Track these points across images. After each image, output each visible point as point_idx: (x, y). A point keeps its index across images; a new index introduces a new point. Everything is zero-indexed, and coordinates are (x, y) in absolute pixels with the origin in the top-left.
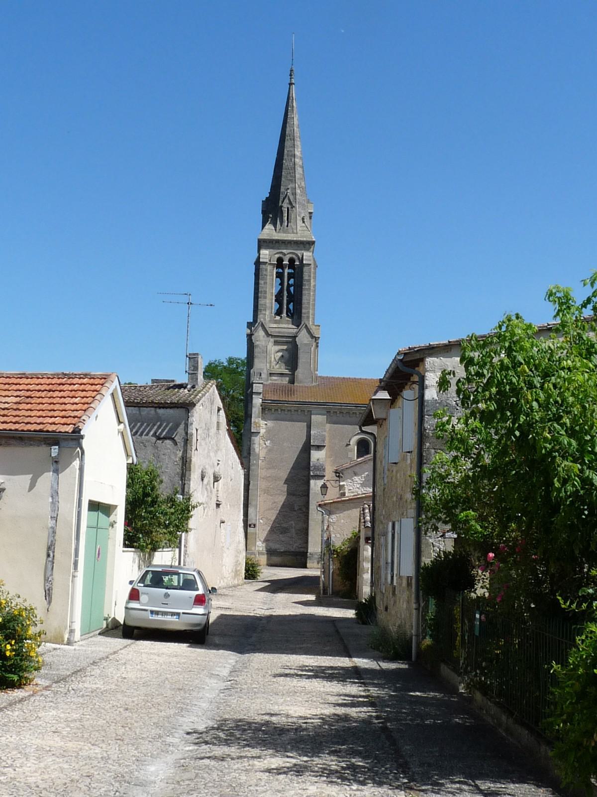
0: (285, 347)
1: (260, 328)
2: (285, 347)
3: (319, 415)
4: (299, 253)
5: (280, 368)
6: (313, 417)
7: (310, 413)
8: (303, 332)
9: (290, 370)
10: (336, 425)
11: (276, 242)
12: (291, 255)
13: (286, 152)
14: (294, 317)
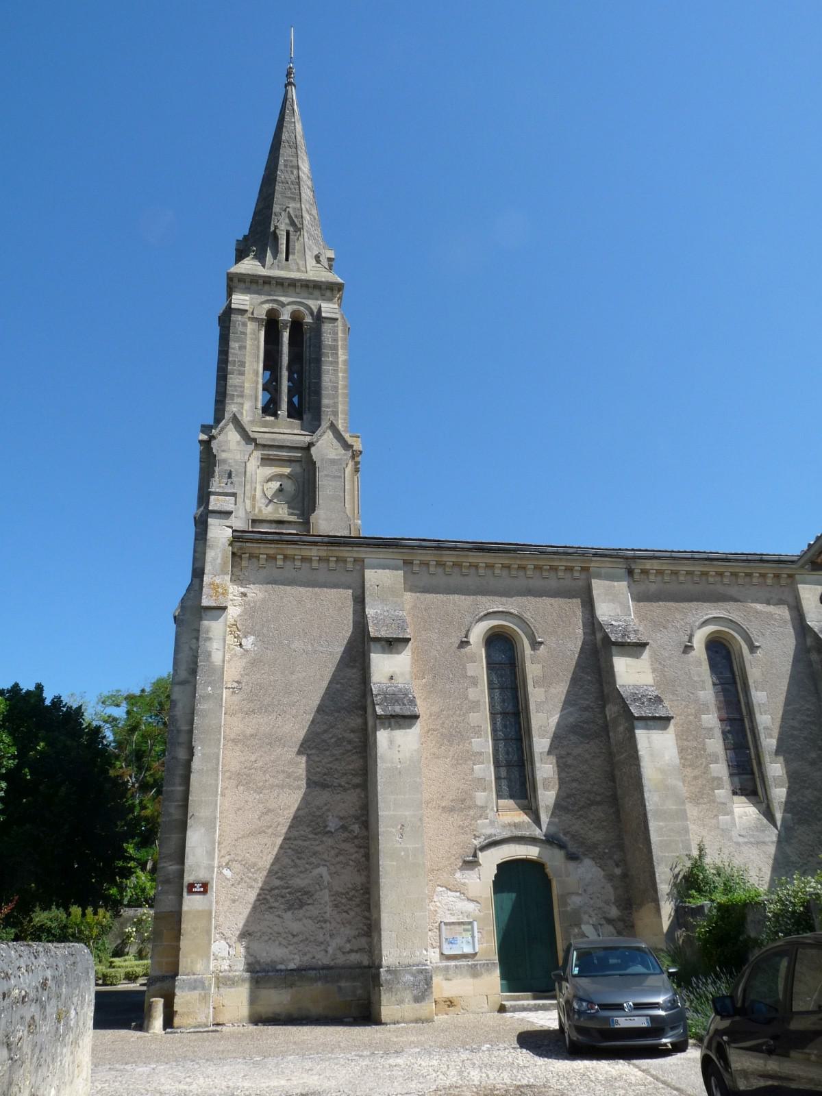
0: (287, 470)
1: (231, 426)
2: (287, 470)
3: (384, 568)
4: (313, 304)
5: (276, 510)
6: (369, 574)
7: (360, 564)
8: (325, 437)
9: (299, 516)
10: (428, 596)
11: (265, 283)
12: (295, 307)
13: (281, 161)
14: (305, 417)
